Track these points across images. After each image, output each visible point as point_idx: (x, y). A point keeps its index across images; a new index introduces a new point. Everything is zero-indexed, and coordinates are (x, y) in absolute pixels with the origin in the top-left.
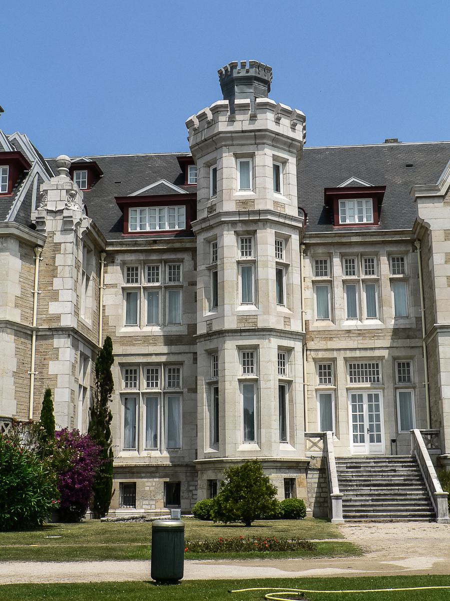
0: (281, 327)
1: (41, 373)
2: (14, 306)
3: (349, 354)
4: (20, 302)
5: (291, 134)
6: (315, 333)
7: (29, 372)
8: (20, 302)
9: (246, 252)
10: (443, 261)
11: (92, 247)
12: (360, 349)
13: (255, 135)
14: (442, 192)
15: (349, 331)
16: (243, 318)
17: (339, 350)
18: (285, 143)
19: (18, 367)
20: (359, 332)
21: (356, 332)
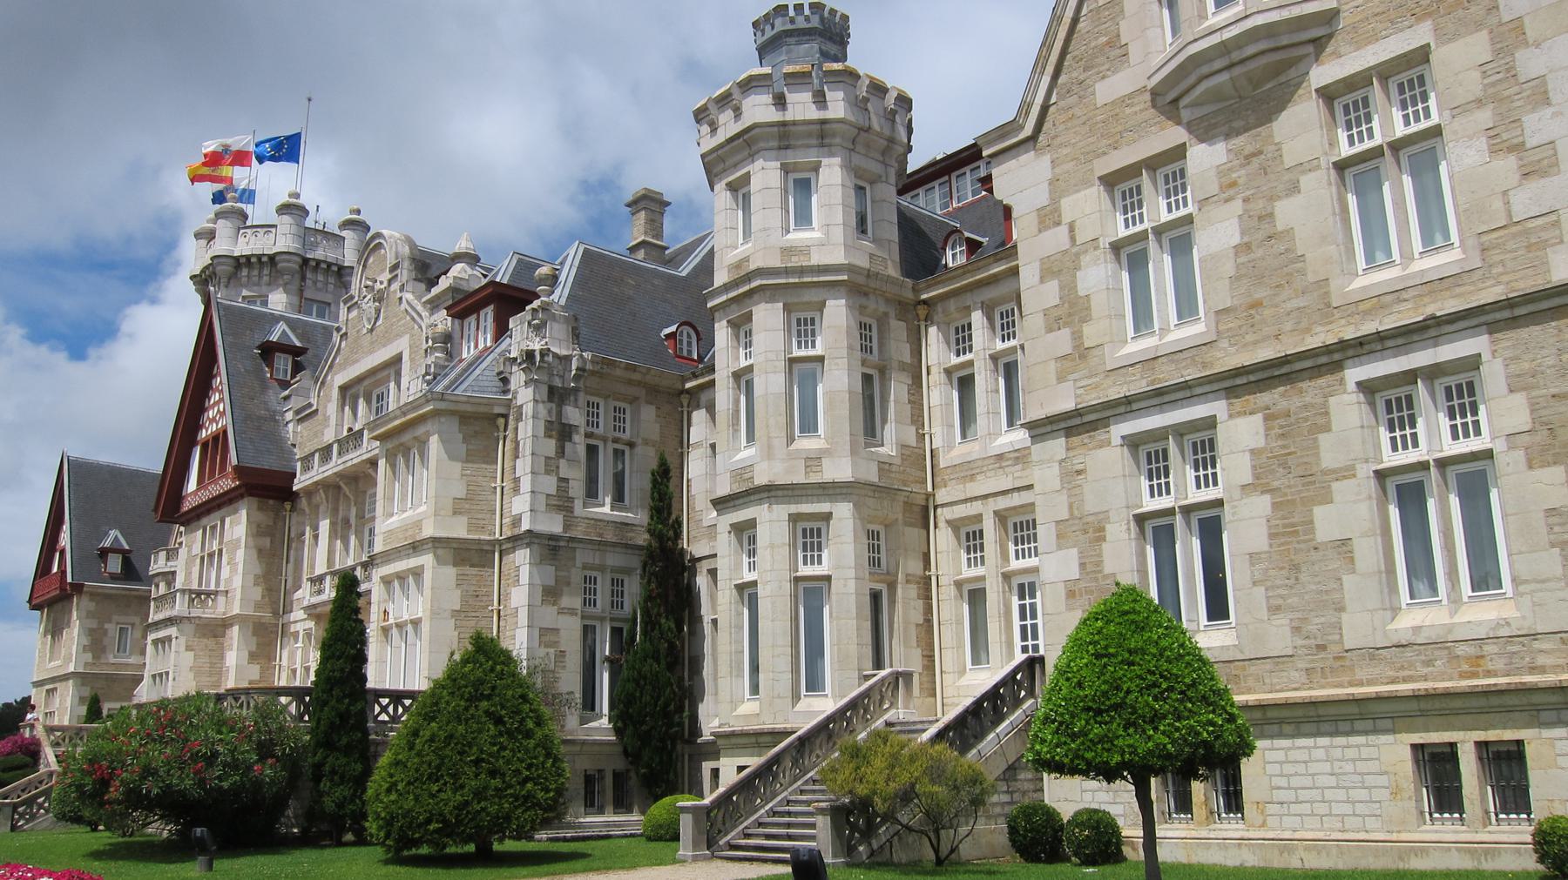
0: (799, 478)
1: (505, 606)
2: (451, 513)
3: (1003, 503)
4: (467, 506)
5: (813, 113)
6: (949, 471)
7: (490, 608)
8: (467, 506)
9: (806, 342)
10: (1037, 278)
11: (642, 393)
12: (1018, 489)
13: (744, 140)
14: (1028, 130)
15: (1000, 457)
16: (741, 473)
17: (986, 497)
18: (810, 135)
19: (464, 601)
20: (1016, 455)
21: (1013, 455)
